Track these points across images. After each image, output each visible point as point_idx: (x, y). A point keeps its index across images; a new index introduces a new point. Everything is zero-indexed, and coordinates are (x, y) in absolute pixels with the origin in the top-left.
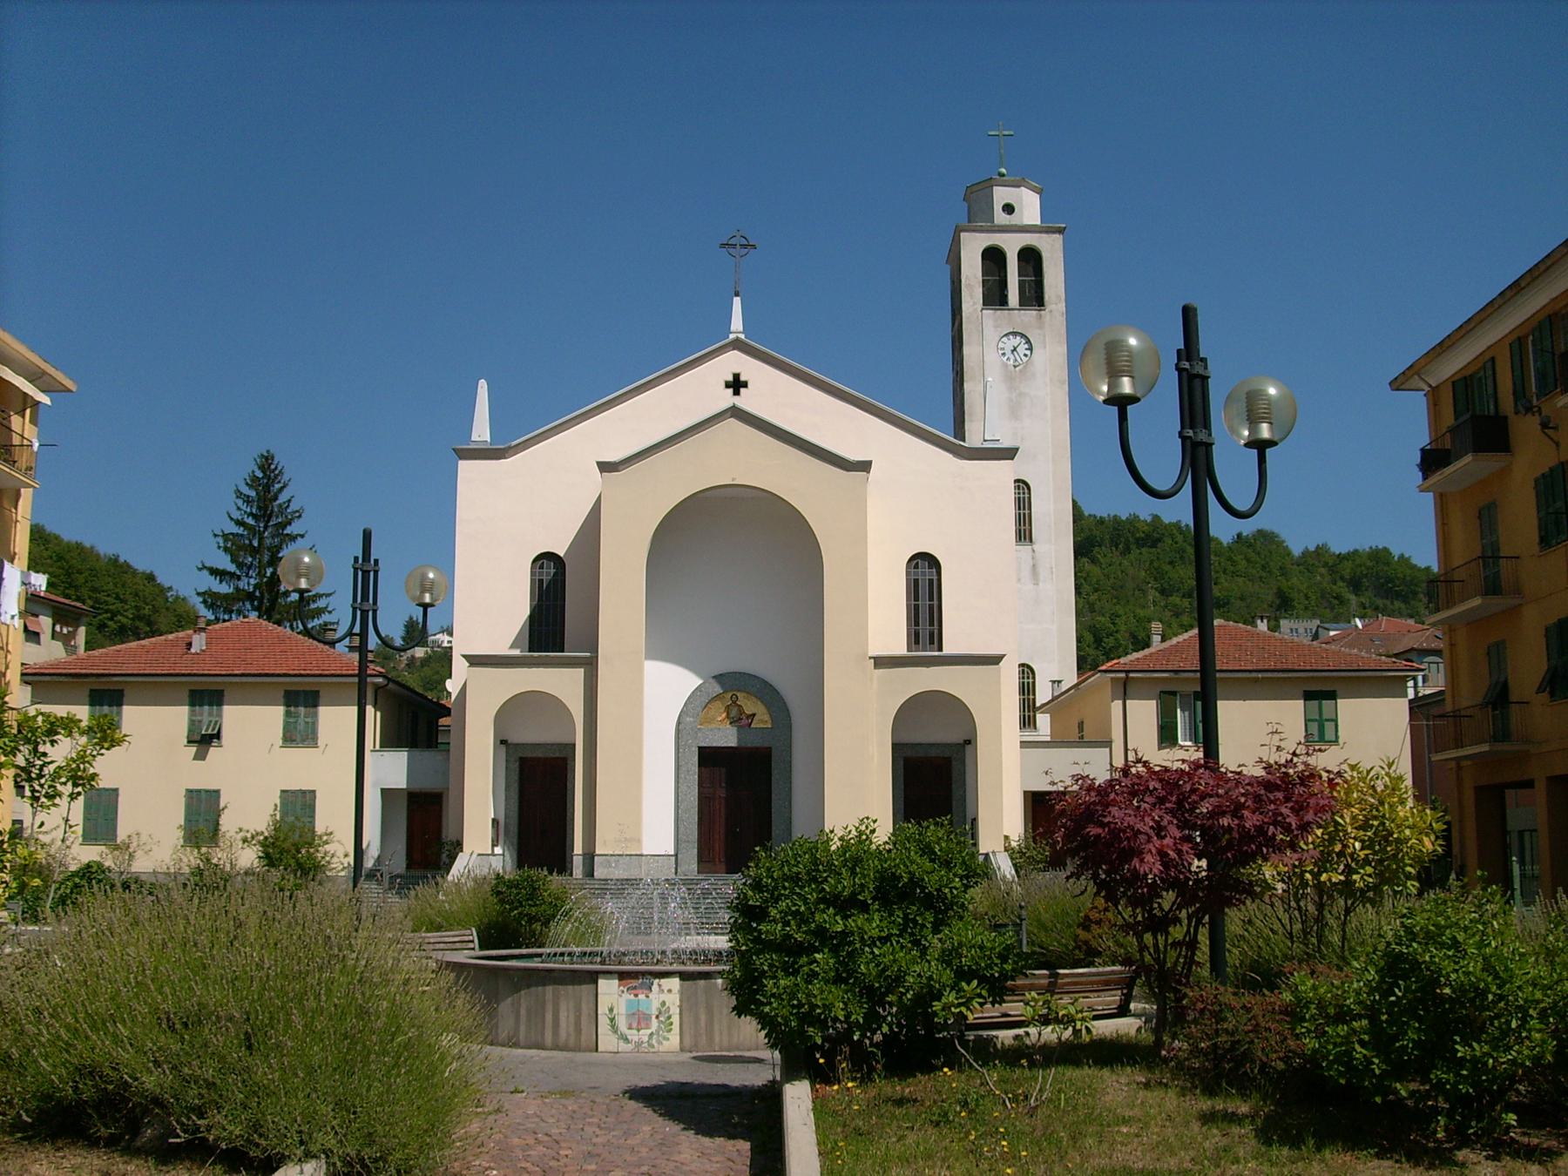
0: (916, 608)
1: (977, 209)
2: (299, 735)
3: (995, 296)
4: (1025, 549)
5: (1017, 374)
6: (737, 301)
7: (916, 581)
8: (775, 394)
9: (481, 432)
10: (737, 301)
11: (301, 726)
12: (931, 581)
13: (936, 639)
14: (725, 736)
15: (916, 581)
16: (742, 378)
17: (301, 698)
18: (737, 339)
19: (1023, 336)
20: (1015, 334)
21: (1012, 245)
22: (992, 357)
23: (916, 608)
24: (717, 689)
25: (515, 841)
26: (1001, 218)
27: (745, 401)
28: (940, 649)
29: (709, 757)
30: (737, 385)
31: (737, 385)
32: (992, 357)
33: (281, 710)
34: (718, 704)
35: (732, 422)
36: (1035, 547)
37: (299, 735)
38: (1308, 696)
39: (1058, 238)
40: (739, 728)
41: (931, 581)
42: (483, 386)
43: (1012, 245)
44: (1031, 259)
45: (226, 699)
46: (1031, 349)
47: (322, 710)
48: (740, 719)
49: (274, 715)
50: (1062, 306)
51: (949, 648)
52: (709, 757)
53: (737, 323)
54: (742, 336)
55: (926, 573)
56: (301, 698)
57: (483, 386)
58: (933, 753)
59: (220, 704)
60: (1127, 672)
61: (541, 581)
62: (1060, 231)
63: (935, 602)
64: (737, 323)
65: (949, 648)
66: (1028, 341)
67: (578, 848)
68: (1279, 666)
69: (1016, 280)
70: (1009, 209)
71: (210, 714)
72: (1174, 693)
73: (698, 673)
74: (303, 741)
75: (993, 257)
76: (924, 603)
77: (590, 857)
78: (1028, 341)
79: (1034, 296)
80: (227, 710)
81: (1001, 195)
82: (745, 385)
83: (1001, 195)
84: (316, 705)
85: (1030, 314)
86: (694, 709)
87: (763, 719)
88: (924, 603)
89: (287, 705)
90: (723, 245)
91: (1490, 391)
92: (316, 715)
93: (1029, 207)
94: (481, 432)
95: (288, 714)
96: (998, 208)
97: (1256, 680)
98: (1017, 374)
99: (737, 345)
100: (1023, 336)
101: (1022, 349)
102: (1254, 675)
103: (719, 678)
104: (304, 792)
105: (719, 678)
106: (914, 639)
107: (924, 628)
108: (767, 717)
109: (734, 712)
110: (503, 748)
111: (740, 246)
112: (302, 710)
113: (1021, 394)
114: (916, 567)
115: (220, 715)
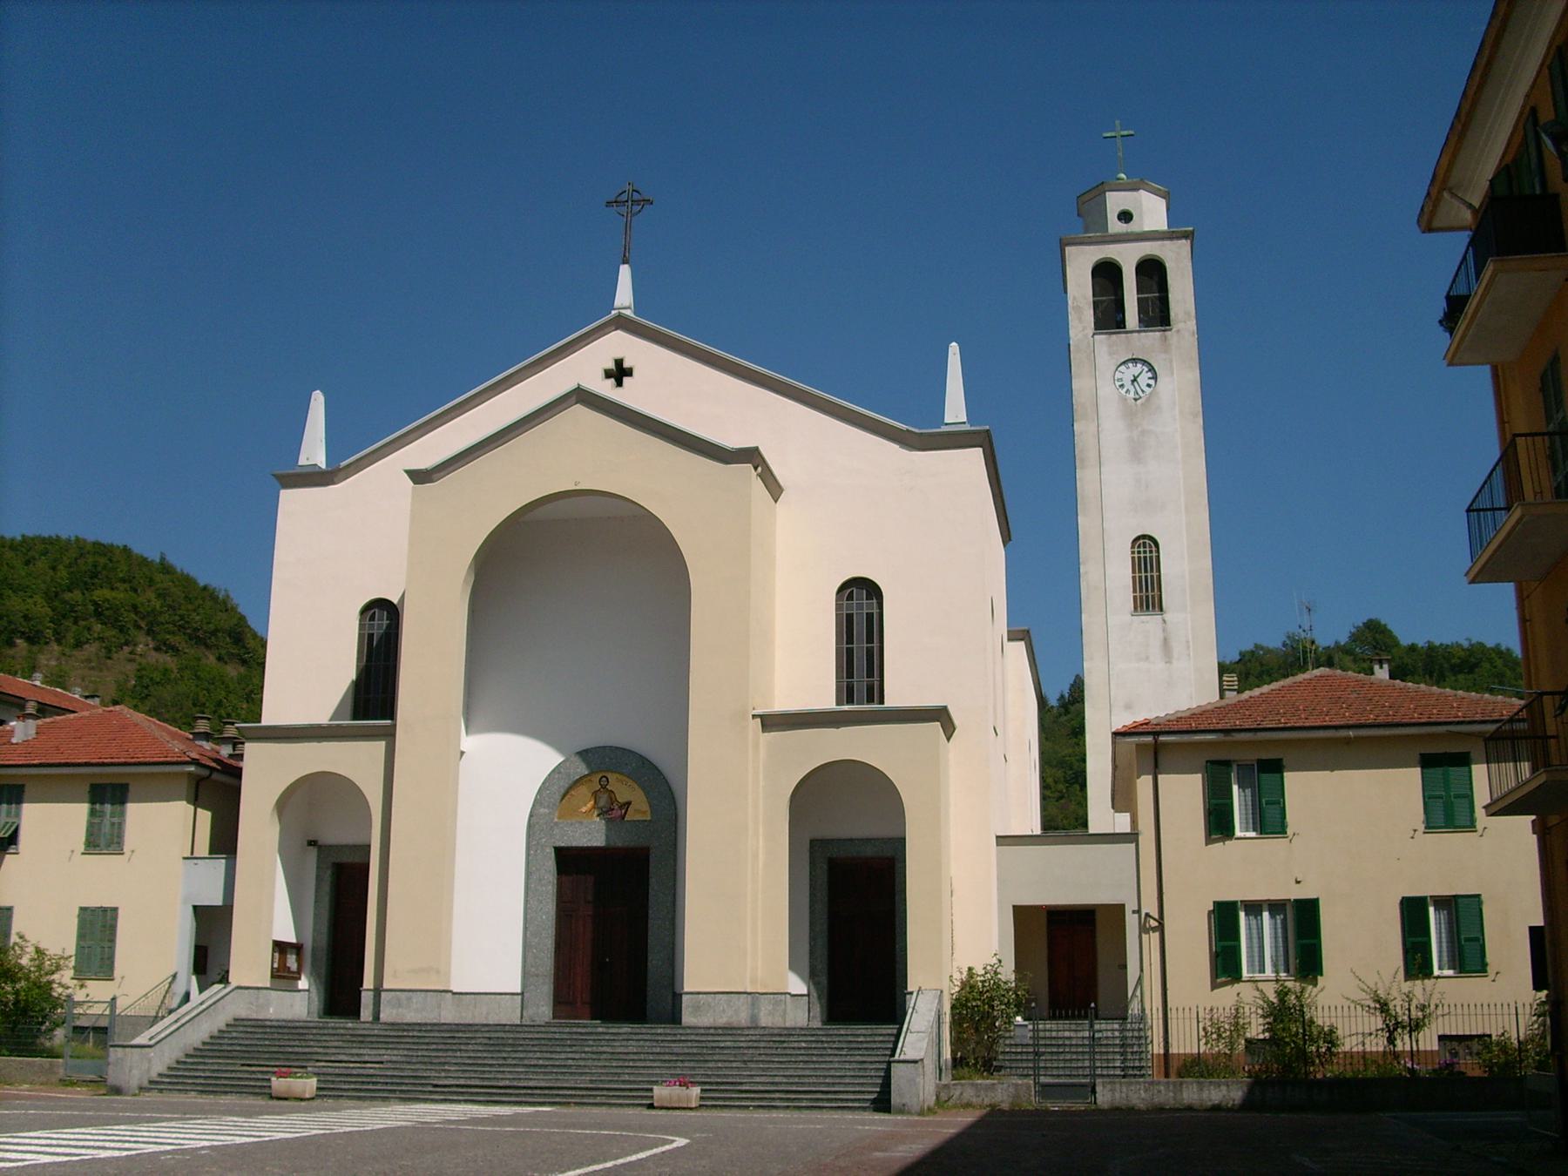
0: (850, 652)
1: (1088, 217)
2: (104, 840)
3: (1109, 318)
4: (1151, 621)
5: (1138, 408)
6: (625, 272)
7: (850, 617)
8: (670, 383)
9: (314, 452)
10: (625, 272)
11: (106, 828)
12: (870, 616)
13: (875, 692)
14: (590, 833)
15: (850, 617)
16: (626, 365)
17: (108, 793)
18: (620, 316)
19: (1144, 362)
20: (1134, 361)
21: (1128, 258)
22: (1107, 391)
23: (850, 652)
24: (582, 769)
25: (323, 971)
26: (1115, 226)
27: (628, 395)
28: (882, 702)
29: (569, 861)
30: (619, 373)
31: (619, 373)
32: (1107, 391)
33: (83, 809)
34: (584, 791)
35: (579, 409)
36: (1167, 616)
37: (104, 840)
38: (1427, 762)
39: (1185, 245)
40: (609, 821)
41: (870, 616)
42: (318, 401)
43: (1128, 258)
44: (1152, 271)
45: (26, 796)
46: (1155, 378)
47: (131, 808)
48: (612, 811)
49: (77, 814)
50: (1192, 325)
51: (890, 702)
52: (569, 861)
53: (624, 296)
54: (628, 313)
55: (861, 605)
56: (108, 793)
57: (318, 401)
58: (869, 851)
59: (19, 801)
60: (1156, 734)
61: (371, 636)
62: (1185, 236)
63: (876, 645)
64: (624, 296)
65: (890, 702)
66: (1152, 369)
67: (368, 982)
68: (1381, 719)
69: (1132, 299)
70: (1126, 216)
71: (8, 814)
72: (1227, 764)
73: (560, 749)
74: (108, 846)
75: (1107, 274)
76: (860, 646)
77: (378, 990)
78: (1152, 369)
79: (1157, 314)
80: (27, 808)
81: (1116, 201)
82: (629, 373)
83: (1116, 201)
84: (123, 802)
85: (1153, 337)
86: (556, 796)
87: (640, 808)
88: (860, 646)
89: (93, 802)
90: (609, 204)
91: (1534, 161)
92: (122, 814)
93: (1152, 211)
94: (314, 452)
95: (92, 813)
96: (1112, 216)
97: (1348, 741)
98: (1138, 408)
99: (622, 323)
100: (1144, 362)
101: (1145, 378)
102: (1343, 733)
103: (584, 754)
104: (104, 910)
105: (584, 754)
106: (847, 693)
107: (861, 681)
108: (646, 807)
109: (603, 801)
110: (313, 852)
111: (631, 202)
112: (108, 807)
113: (1143, 432)
114: (850, 597)
115: (18, 815)
